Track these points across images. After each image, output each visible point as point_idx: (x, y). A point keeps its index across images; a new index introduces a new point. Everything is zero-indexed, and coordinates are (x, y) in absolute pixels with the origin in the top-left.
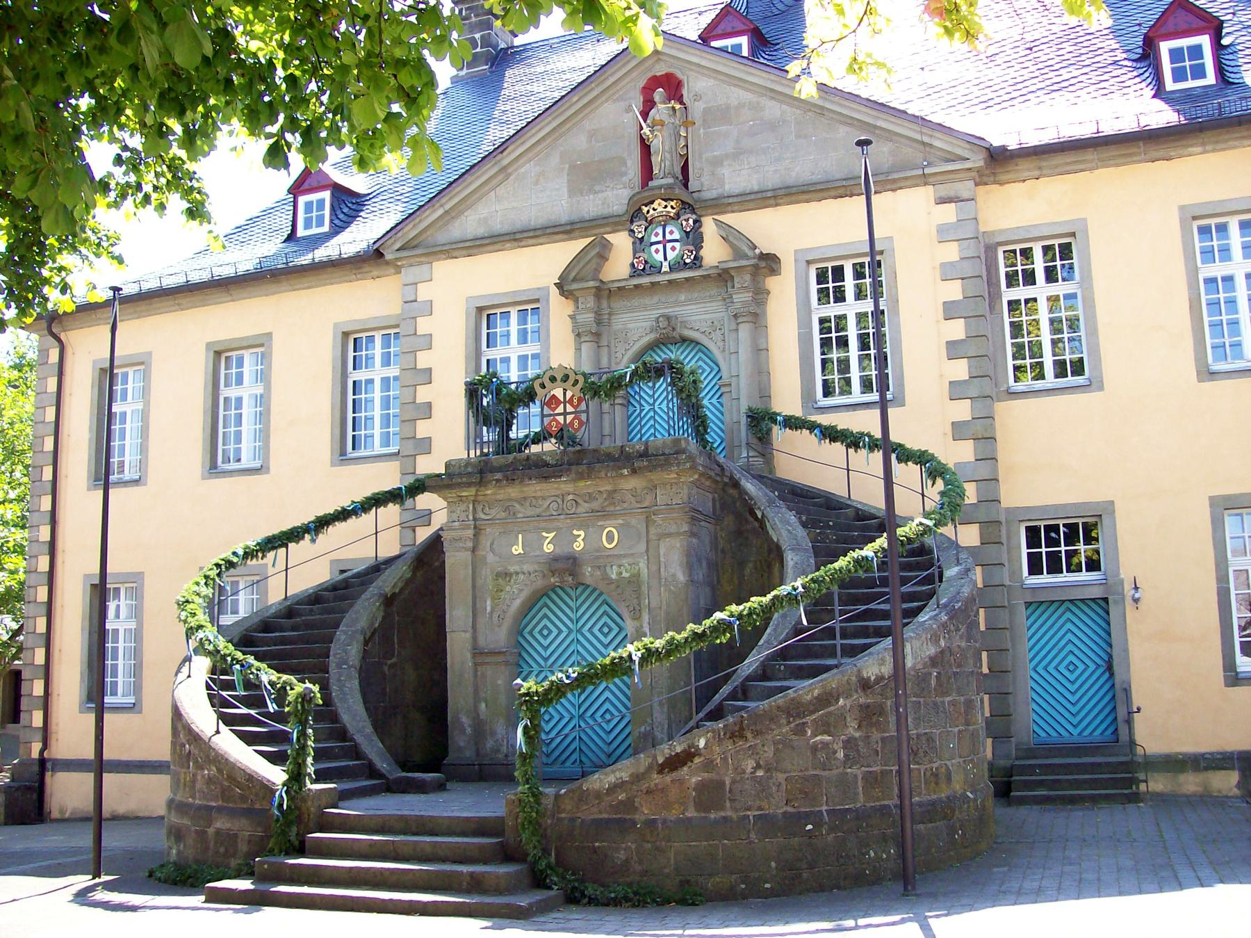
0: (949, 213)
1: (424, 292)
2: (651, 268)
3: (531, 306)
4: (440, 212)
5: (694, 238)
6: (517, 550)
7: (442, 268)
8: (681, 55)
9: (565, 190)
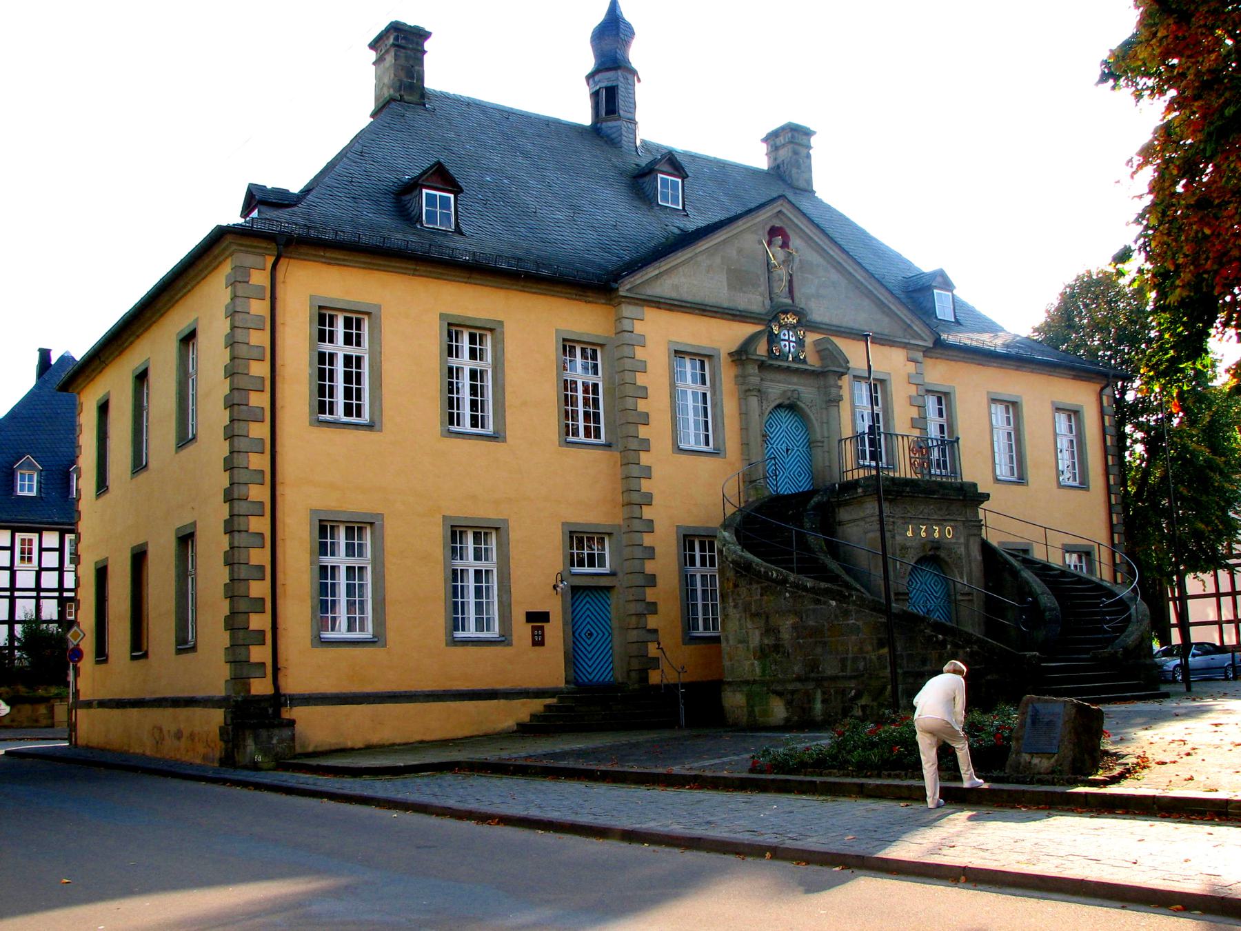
0: (911, 367)
1: (639, 328)
2: (783, 356)
3: (702, 358)
4: (657, 272)
5: (800, 343)
6: (909, 534)
7: (650, 314)
8: (796, 221)
9: (725, 284)
